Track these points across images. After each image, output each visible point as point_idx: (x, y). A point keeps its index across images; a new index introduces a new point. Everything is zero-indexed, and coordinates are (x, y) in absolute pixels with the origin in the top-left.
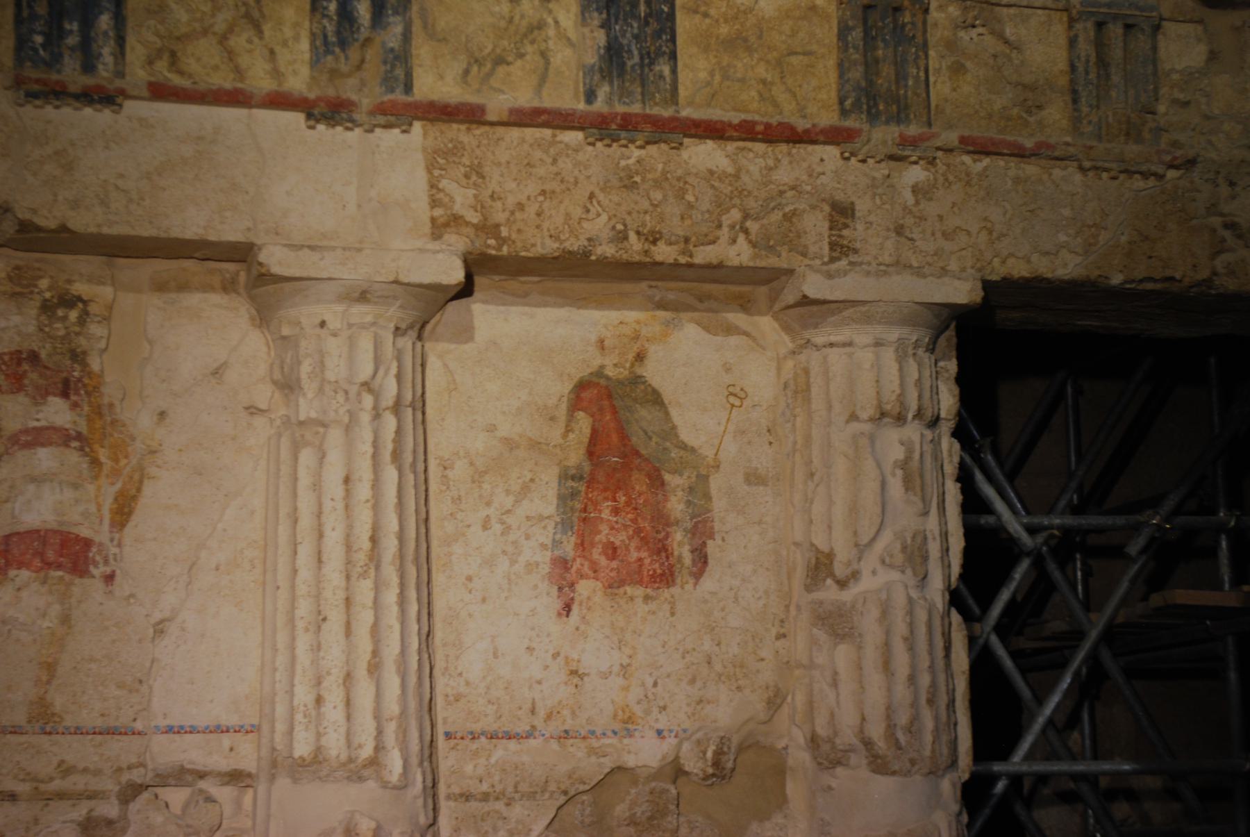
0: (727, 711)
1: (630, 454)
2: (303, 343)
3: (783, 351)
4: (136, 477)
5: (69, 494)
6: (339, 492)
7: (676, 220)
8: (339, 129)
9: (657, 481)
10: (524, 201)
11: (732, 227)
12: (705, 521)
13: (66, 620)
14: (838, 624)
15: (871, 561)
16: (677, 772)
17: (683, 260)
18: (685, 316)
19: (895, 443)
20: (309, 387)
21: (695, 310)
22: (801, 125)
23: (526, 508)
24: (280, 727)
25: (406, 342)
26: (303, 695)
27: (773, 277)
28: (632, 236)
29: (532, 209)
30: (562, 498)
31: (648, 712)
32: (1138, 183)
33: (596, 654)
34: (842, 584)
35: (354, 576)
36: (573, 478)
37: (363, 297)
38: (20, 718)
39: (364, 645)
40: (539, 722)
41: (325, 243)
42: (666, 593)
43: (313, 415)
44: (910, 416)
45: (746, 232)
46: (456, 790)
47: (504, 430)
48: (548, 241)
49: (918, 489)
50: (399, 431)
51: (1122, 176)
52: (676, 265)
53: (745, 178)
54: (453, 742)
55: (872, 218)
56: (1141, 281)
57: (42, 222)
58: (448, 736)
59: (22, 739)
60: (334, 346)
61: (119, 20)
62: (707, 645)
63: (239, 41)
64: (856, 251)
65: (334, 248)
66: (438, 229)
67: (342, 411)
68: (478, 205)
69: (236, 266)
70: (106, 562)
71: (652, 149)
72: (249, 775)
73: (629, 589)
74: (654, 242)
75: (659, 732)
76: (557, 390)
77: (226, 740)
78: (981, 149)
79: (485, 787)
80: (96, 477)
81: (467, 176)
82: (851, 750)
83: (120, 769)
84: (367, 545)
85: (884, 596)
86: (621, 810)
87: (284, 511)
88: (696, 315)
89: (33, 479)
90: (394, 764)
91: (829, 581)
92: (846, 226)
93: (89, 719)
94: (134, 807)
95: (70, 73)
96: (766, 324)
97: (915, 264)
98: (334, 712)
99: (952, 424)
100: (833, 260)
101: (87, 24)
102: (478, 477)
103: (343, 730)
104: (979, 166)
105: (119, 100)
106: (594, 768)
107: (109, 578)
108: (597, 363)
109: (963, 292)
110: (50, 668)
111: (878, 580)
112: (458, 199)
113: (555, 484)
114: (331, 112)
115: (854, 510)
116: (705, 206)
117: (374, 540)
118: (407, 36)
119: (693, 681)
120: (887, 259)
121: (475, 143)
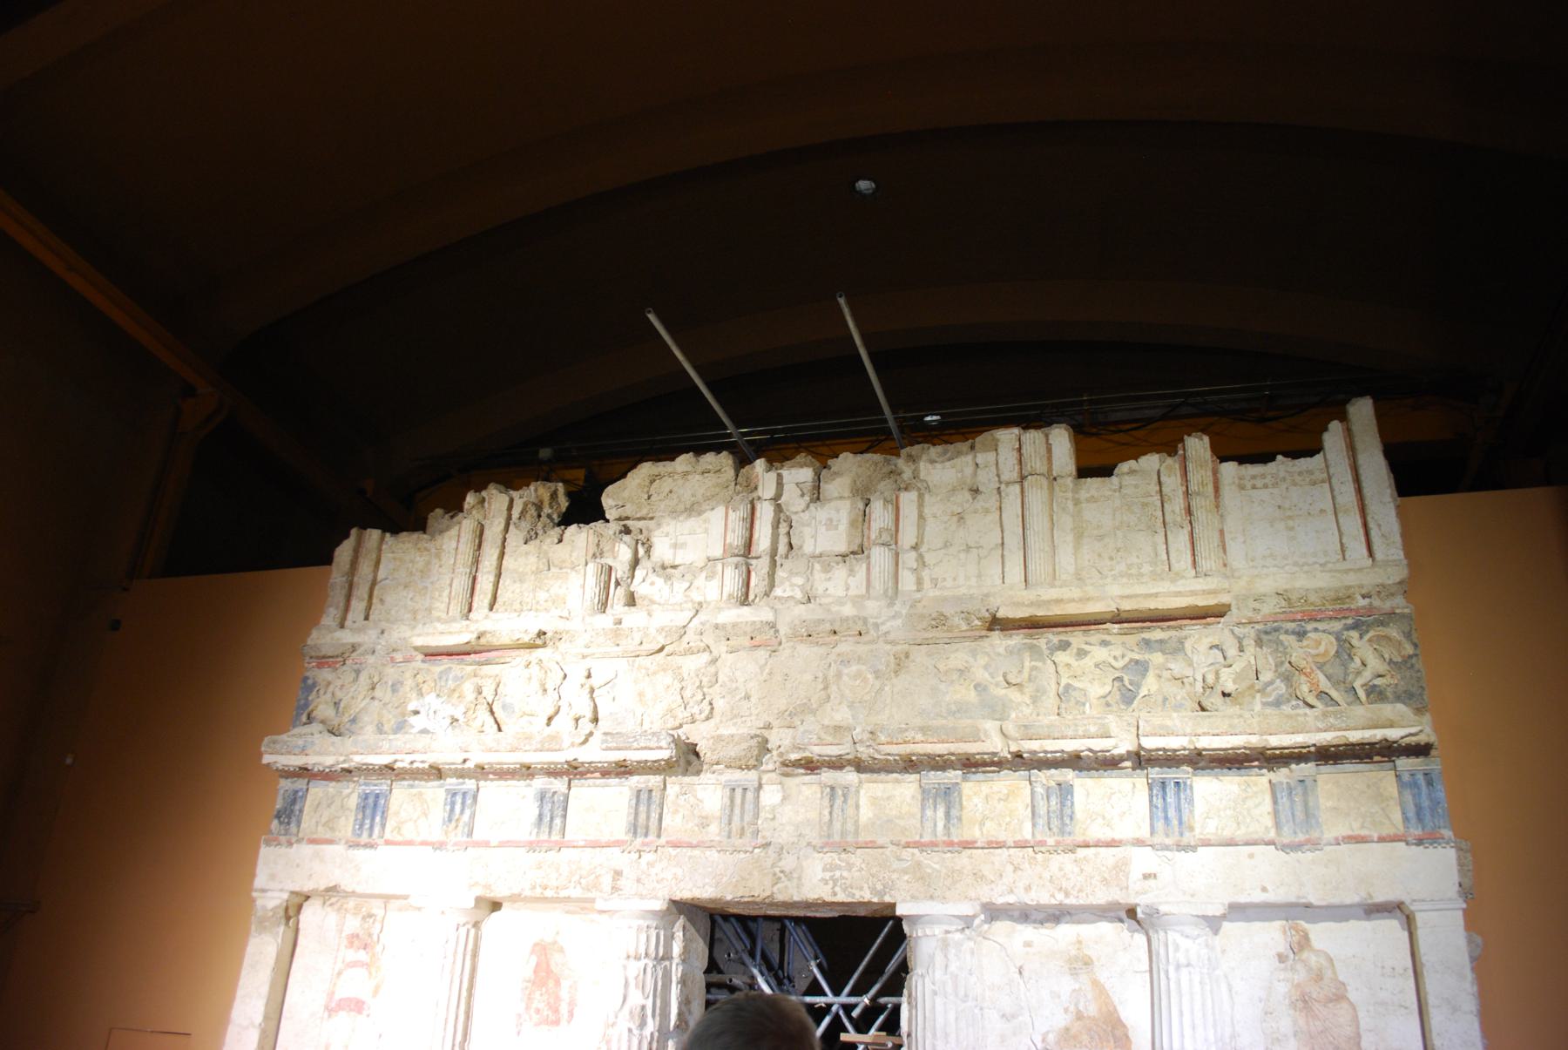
1: (549, 972)
9: (558, 983)
19: (635, 967)
22: (605, 838)
32: (742, 855)
61: (384, 818)
78: (676, 845)
95: (364, 838)
101: (373, 819)
114: (439, 846)
118: (473, 816)
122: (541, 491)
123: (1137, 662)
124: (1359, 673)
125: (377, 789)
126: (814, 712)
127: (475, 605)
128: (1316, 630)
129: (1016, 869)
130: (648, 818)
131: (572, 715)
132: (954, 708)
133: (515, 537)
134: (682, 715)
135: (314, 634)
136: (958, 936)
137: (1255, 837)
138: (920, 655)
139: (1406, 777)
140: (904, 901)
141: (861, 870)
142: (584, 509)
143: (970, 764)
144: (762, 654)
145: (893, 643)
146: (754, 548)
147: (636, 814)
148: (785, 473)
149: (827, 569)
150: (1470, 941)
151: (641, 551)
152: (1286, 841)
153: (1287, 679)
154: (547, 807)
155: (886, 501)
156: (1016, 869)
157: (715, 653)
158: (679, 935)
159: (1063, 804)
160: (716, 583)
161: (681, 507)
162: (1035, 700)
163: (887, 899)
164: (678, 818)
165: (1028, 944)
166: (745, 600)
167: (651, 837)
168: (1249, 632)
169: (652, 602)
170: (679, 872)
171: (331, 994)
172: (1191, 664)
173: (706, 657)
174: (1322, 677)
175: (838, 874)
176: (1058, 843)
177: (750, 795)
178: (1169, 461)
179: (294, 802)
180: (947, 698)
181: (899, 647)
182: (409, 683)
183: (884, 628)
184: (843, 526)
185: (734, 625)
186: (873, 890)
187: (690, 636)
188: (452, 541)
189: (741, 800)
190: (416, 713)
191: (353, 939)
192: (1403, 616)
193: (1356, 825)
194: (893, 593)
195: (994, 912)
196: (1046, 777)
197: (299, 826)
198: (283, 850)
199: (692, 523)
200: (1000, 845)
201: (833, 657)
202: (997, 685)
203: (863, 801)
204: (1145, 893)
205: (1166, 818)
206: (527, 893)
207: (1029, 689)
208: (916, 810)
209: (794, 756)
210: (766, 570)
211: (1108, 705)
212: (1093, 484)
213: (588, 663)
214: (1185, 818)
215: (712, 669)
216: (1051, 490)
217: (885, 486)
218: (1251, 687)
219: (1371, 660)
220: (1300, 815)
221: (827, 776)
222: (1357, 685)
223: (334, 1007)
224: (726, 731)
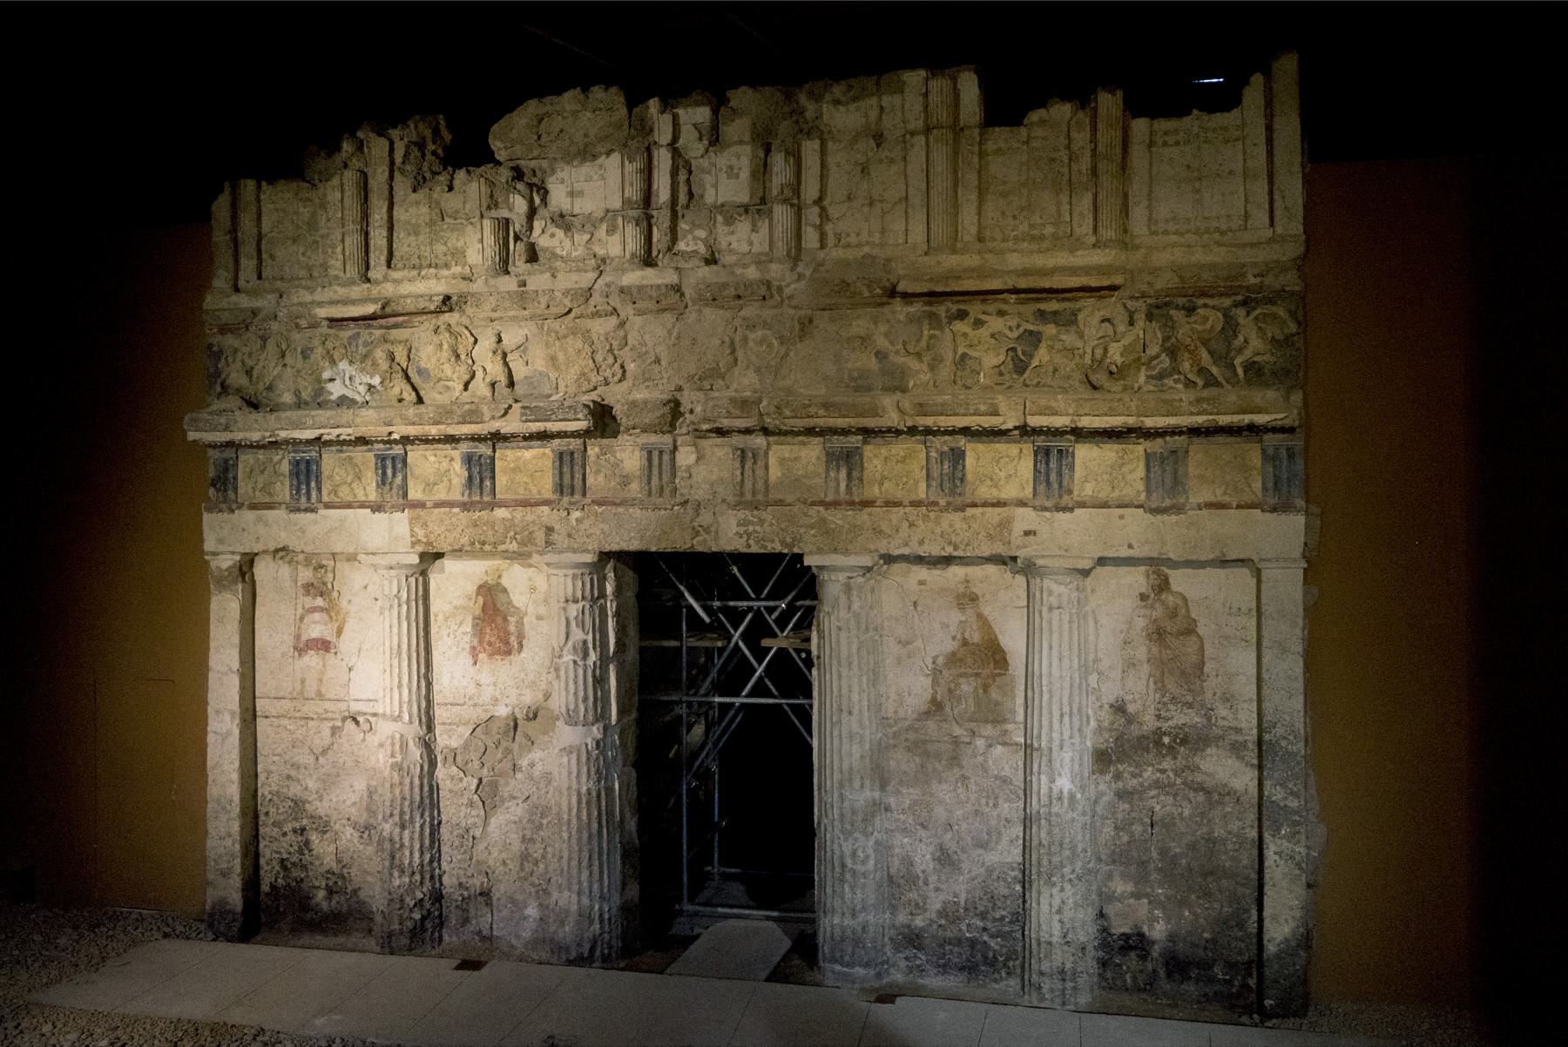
0: (529, 698)
1: (496, 610)
9: (505, 620)
19: (574, 610)
33: (485, 678)
63: (354, 485)
66: (413, 544)
78: (600, 504)
93: (331, 696)
101: (308, 485)
102: (446, 619)
106: (485, 716)
114: (377, 508)
118: (405, 478)
122: (421, 126)
123: (1031, 333)
124: (1240, 351)
125: (307, 456)
126: (723, 377)
127: (372, 263)
128: (1205, 306)
129: (911, 525)
130: (572, 478)
131: (488, 380)
132: (855, 374)
133: (402, 186)
134: (595, 379)
135: (209, 298)
136: (860, 580)
137: (1127, 500)
138: (823, 322)
139: (1270, 452)
140: (811, 553)
141: (771, 525)
142: (468, 152)
143: (867, 433)
144: (669, 318)
145: (795, 308)
146: (653, 199)
147: (561, 474)
148: (681, 112)
149: (729, 221)
150: (1306, 593)
151: (537, 200)
152: (1154, 506)
153: (1173, 353)
154: (476, 471)
155: (787, 153)
156: (911, 525)
157: (623, 315)
159: (955, 468)
160: (617, 238)
161: (573, 149)
162: (932, 368)
163: (796, 550)
164: (601, 478)
165: (921, 583)
166: (648, 261)
167: (577, 497)
168: (1141, 305)
169: (555, 255)
171: (298, 637)
172: (1082, 337)
173: (613, 321)
174: (1204, 354)
175: (751, 528)
176: (949, 504)
177: (666, 457)
178: (1081, 114)
179: (226, 470)
180: (849, 365)
181: (803, 312)
182: (320, 351)
183: (787, 291)
184: (745, 174)
185: (640, 288)
186: (783, 543)
187: (597, 298)
188: (338, 193)
189: (659, 464)
190: (332, 380)
191: (309, 588)
192: (1292, 293)
193: (1219, 492)
194: (796, 254)
195: (889, 559)
196: (938, 443)
197: (236, 489)
199: (586, 169)
200: (897, 504)
201: (737, 322)
202: (897, 352)
203: (772, 461)
204: (1025, 547)
205: (1048, 483)
207: (927, 358)
208: (821, 470)
209: (705, 427)
210: (667, 224)
211: (1001, 374)
212: (1001, 137)
213: (498, 326)
214: (1065, 483)
215: (622, 333)
216: (956, 141)
217: (785, 127)
218: (1139, 359)
219: (1253, 342)
220: (1168, 482)
221: (737, 440)
222: (1237, 362)
224: (639, 396)
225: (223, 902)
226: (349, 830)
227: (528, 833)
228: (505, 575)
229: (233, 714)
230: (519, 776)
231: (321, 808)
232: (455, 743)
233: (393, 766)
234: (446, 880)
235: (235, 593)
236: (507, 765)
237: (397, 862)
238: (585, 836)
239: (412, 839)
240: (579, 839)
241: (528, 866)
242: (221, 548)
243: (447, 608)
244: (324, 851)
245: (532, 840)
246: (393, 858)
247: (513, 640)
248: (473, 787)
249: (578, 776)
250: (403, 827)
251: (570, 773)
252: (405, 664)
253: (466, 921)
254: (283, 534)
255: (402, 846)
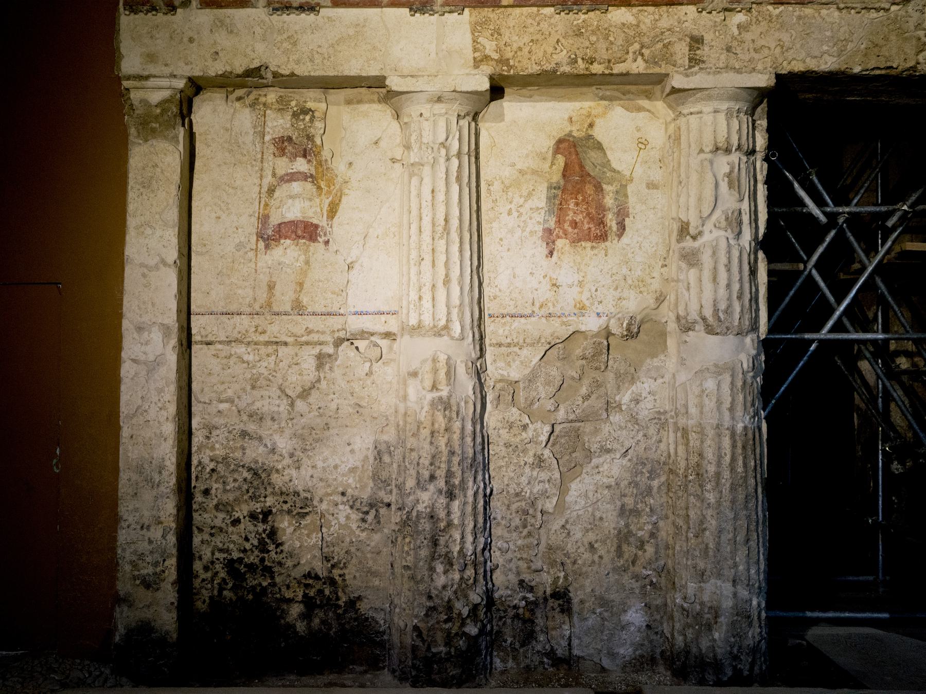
0: (634, 304)
1: (585, 176)
2: (413, 125)
3: (669, 119)
4: (339, 194)
5: (307, 203)
6: (430, 197)
7: (604, 51)
8: (427, 15)
9: (599, 188)
10: (522, 46)
11: (635, 53)
12: (624, 208)
13: (307, 262)
14: (691, 259)
15: (709, 225)
16: (608, 334)
17: (607, 72)
18: (614, 102)
19: (723, 164)
20: (415, 147)
21: (621, 99)
23: (530, 204)
24: (405, 311)
25: (464, 123)
26: (413, 296)
27: (661, 79)
28: (580, 61)
29: (526, 50)
30: (549, 199)
31: (592, 304)
34: (694, 238)
35: (437, 237)
36: (555, 188)
37: (439, 99)
38: (288, 308)
39: (441, 271)
40: (536, 309)
41: (420, 73)
42: (603, 245)
43: (417, 160)
44: (734, 149)
45: (642, 55)
46: (494, 341)
47: (519, 167)
48: (534, 66)
49: (736, 187)
50: (460, 166)
51: (863, 11)
52: (603, 74)
53: (642, 26)
54: (492, 319)
55: (713, 43)
56: (873, 69)
57: (283, 72)
58: (490, 316)
59: (290, 317)
60: (426, 125)
62: (625, 271)
64: (703, 62)
65: (423, 76)
66: (477, 63)
67: (430, 158)
68: (498, 50)
69: (375, 86)
70: (325, 235)
71: (591, 14)
72: (394, 334)
73: (583, 243)
74: (591, 63)
75: (598, 314)
76: (547, 144)
77: (383, 318)
79: (509, 340)
80: (320, 195)
81: (492, 35)
82: (695, 322)
83: (334, 331)
84: (443, 223)
85: (714, 244)
86: (578, 352)
87: (406, 208)
88: (622, 102)
89: (291, 197)
90: (456, 329)
91: (688, 237)
92: (698, 48)
93: (319, 309)
94: (340, 348)
96: (659, 106)
97: (737, 67)
98: (427, 304)
99: (763, 154)
100: (690, 67)
102: (506, 189)
103: (431, 312)
104: (777, 11)
105: (317, 9)
106: (564, 332)
107: (327, 243)
108: (567, 130)
109: (764, 80)
110: (301, 284)
111: (714, 236)
112: (488, 47)
113: (545, 191)
115: (700, 199)
116: (620, 42)
117: (446, 220)
119: (616, 289)
120: (721, 65)
121: (496, 17)
158: (763, 123)
170: (785, 37)
171: (264, 219)
191: (283, 145)
198: (160, 18)
206: (567, 69)
223: (272, 234)
225: (145, 628)
226: (344, 511)
227: (629, 501)
228: (599, 122)
229: (166, 329)
230: (616, 418)
231: (298, 479)
232: (515, 374)
233: (433, 404)
234: (499, 578)
235: (175, 139)
236: (596, 403)
237: (442, 550)
238: (741, 497)
239: (463, 514)
240: (733, 502)
241: (629, 551)
242: (152, 69)
243: (507, 172)
244: (302, 545)
245: (636, 512)
246: (435, 543)
247: (611, 221)
248: (544, 438)
249: (732, 409)
250: (451, 496)
251: (719, 403)
252: (455, 248)
253: (529, 637)
254: (260, 47)
255: (450, 524)
